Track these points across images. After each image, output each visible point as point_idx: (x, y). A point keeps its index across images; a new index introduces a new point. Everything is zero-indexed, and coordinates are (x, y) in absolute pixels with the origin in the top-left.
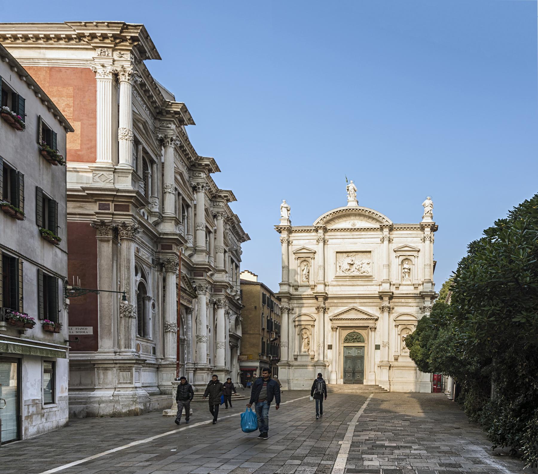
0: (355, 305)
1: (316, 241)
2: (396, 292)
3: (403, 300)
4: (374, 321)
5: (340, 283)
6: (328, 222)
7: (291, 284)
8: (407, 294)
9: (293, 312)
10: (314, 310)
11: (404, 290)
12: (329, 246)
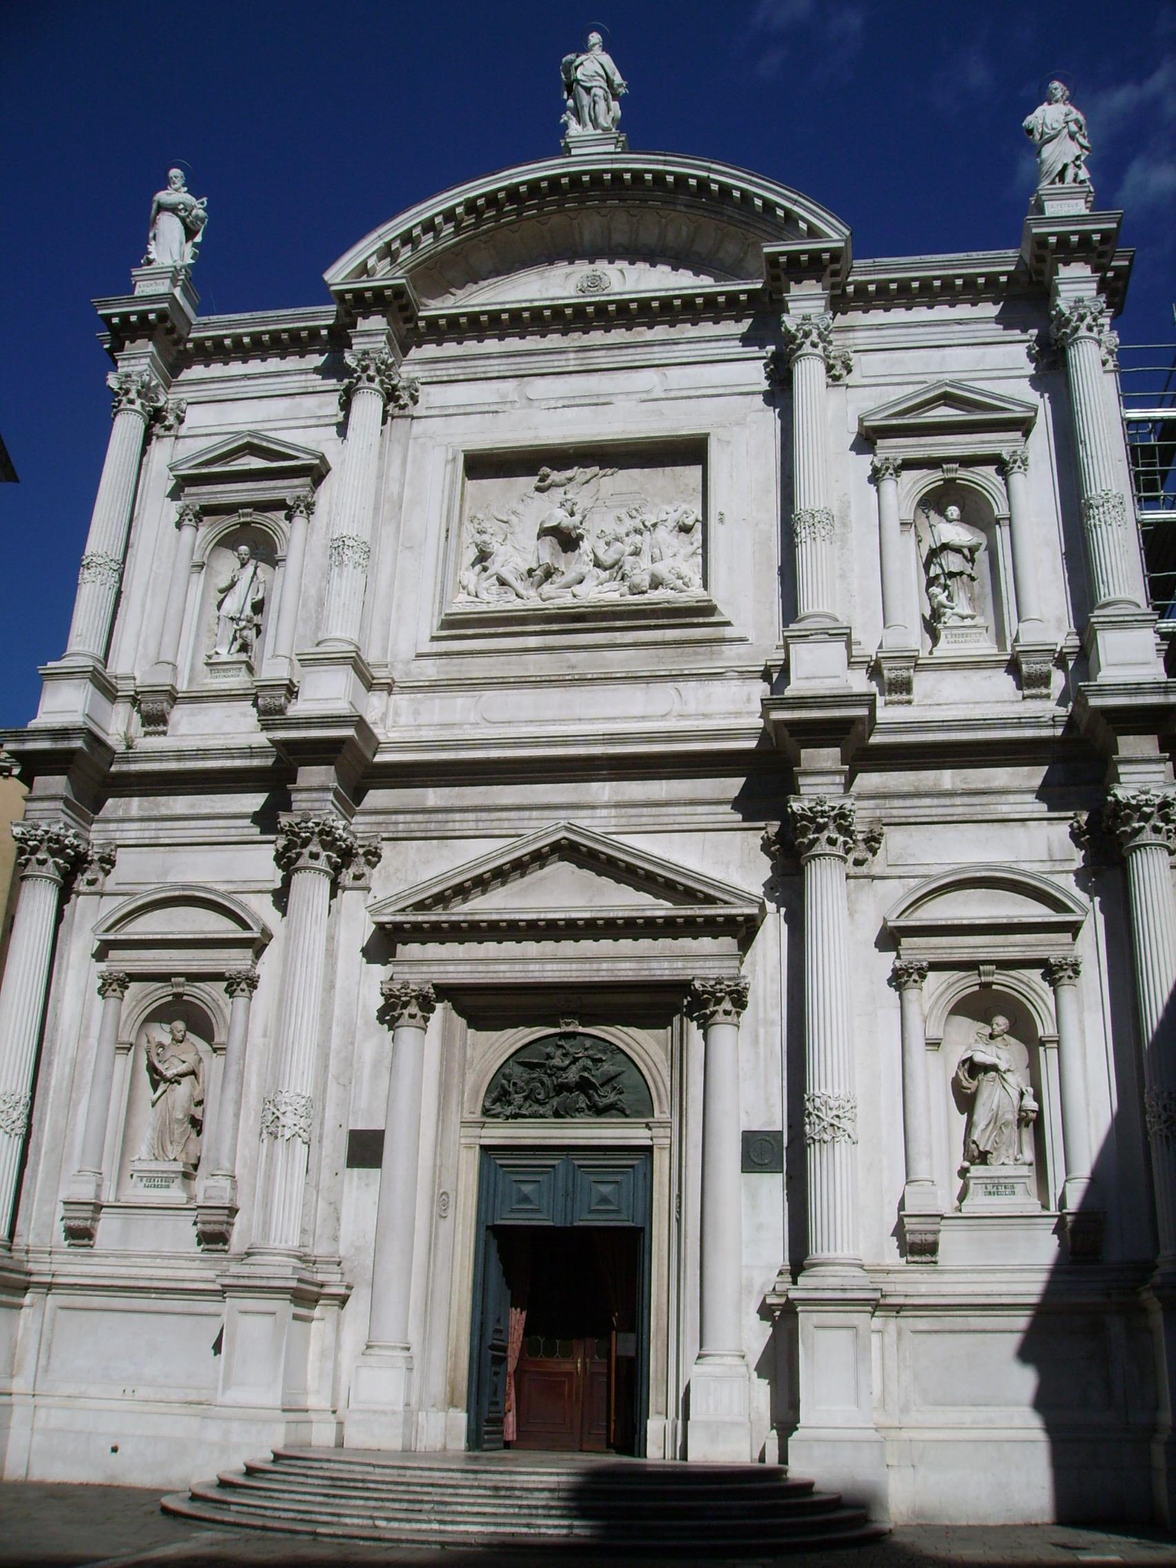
3: (947, 778)
4: (727, 944)
7: (126, 688)
9: (109, 883)
10: (260, 863)
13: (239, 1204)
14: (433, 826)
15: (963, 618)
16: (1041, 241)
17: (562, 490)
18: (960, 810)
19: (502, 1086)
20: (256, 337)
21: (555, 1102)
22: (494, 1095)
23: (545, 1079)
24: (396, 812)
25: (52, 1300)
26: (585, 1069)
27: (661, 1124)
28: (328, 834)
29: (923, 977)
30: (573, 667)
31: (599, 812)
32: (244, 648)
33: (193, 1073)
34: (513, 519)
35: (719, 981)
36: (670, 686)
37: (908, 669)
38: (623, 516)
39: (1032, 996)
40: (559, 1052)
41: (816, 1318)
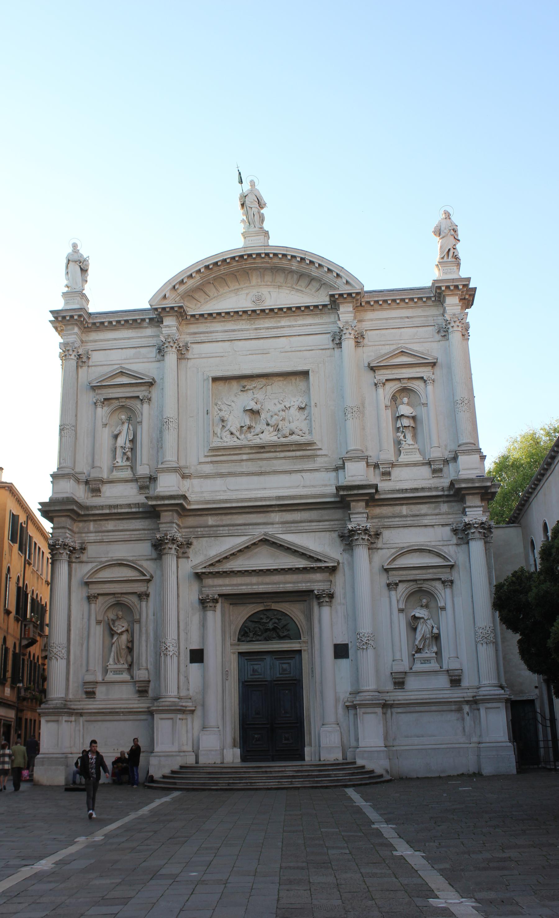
0: (270, 530)
1: (154, 350)
2: (383, 486)
3: (404, 510)
5: (224, 469)
6: (190, 295)
8: (416, 490)
9: (84, 558)
10: (144, 549)
11: (410, 477)
12: (190, 363)
13: (151, 679)
14: (212, 532)
15: (409, 445)
16: (440, 288)
17: (251, 391)
18: (409, 522)
19: (245, 630)
20: (118, 322)
21: (265, 635)
22: (242, 633)
23: (261, 627)
24: (197, 527)
25: (81, 719)
26: (275, 623)
27: (304, 642)
28: (175, 540)
29: (398, 585)
30: (261, 467)
31: (275, 526)
32: (128, 459)
33: (127, 630)
34: (233, 404)
35: (324, 591)
36: (299, 475)
37: (389, 468)
38: (277, 403)
40: (265, 617)
41: (363, 710)
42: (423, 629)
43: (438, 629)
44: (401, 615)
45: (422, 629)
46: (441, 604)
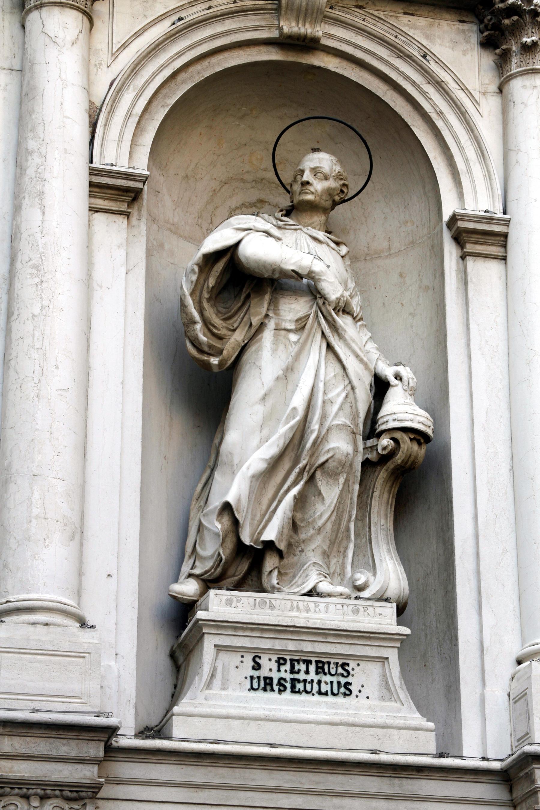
39: (433, 101)
42: (286, 383)
43: (436, 400)
44: (111, 231)
45: (289, 372)
46: (472, 196)
